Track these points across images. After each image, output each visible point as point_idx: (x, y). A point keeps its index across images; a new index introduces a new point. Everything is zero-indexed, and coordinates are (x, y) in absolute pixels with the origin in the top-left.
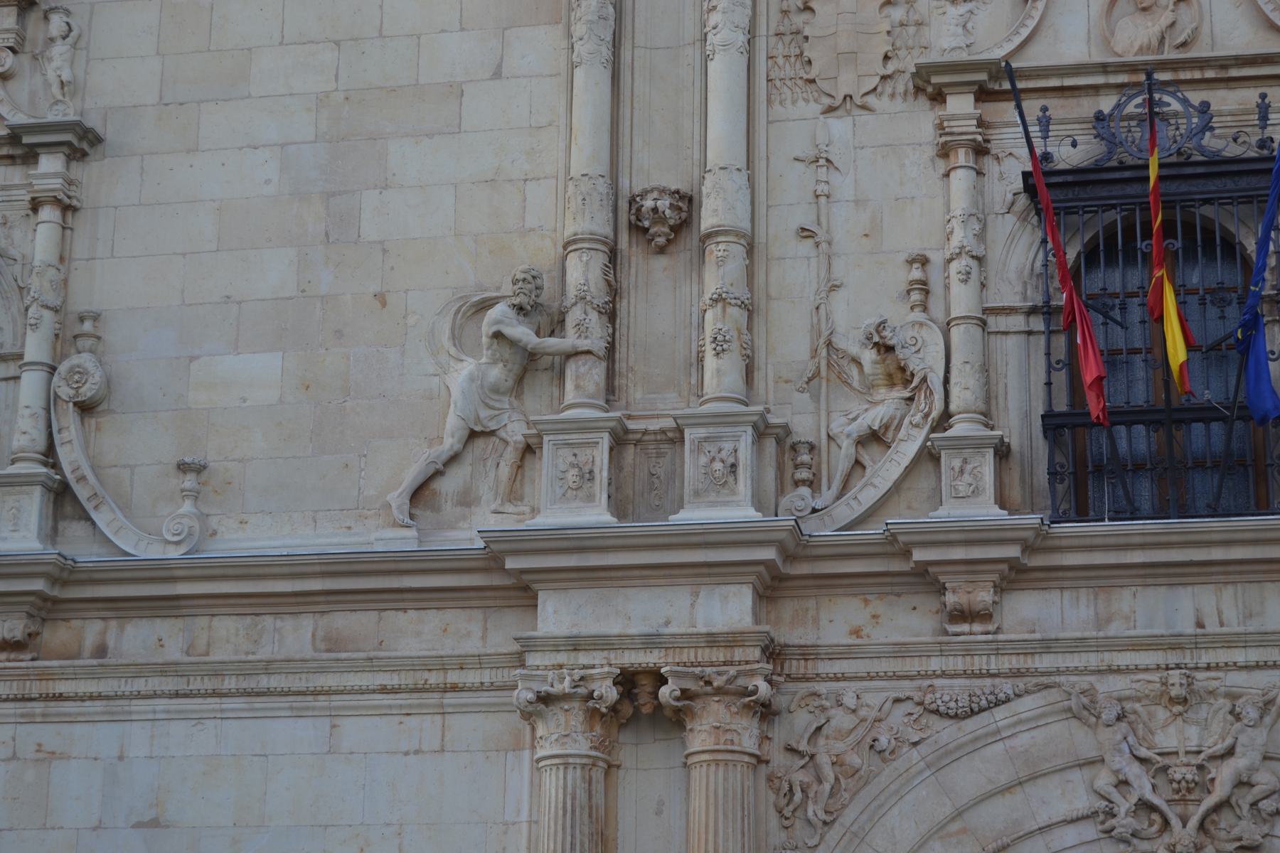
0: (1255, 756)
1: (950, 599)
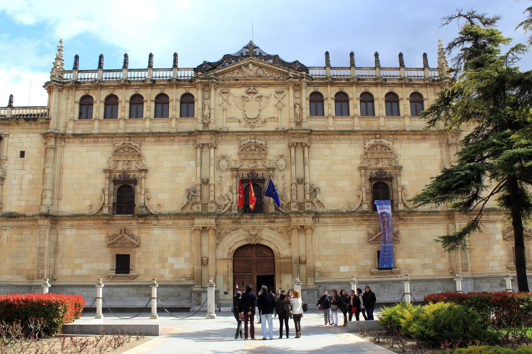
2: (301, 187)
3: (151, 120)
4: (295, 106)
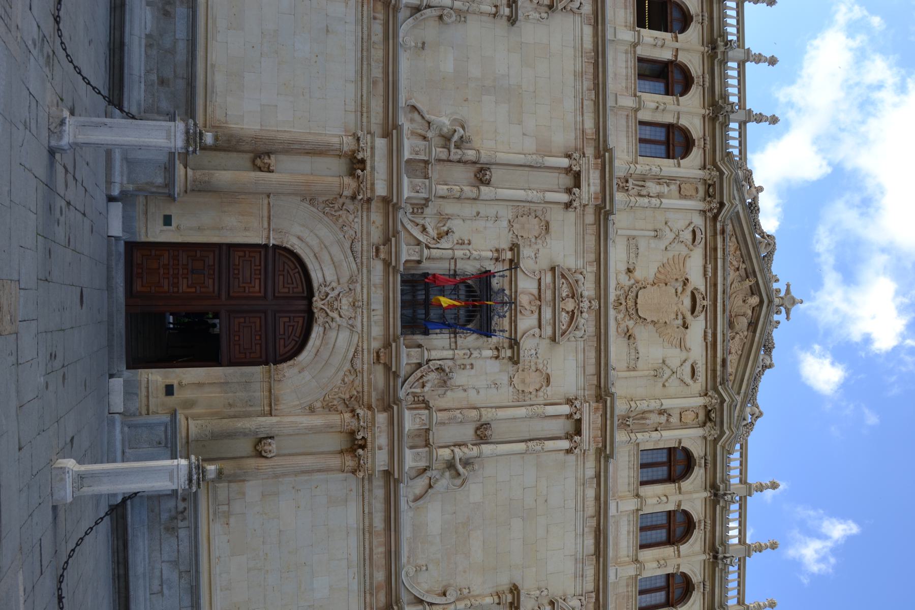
0: (340, 323)
1: (382, 247)
2: (467, 433)
3: (635, 45)
4: (661, 412)
